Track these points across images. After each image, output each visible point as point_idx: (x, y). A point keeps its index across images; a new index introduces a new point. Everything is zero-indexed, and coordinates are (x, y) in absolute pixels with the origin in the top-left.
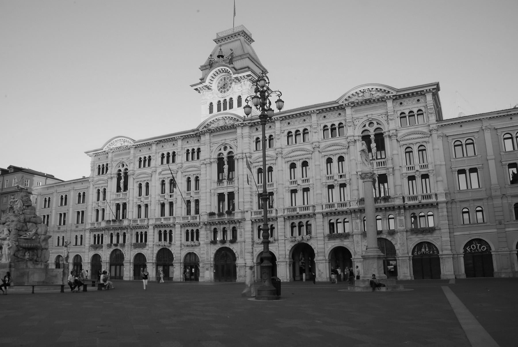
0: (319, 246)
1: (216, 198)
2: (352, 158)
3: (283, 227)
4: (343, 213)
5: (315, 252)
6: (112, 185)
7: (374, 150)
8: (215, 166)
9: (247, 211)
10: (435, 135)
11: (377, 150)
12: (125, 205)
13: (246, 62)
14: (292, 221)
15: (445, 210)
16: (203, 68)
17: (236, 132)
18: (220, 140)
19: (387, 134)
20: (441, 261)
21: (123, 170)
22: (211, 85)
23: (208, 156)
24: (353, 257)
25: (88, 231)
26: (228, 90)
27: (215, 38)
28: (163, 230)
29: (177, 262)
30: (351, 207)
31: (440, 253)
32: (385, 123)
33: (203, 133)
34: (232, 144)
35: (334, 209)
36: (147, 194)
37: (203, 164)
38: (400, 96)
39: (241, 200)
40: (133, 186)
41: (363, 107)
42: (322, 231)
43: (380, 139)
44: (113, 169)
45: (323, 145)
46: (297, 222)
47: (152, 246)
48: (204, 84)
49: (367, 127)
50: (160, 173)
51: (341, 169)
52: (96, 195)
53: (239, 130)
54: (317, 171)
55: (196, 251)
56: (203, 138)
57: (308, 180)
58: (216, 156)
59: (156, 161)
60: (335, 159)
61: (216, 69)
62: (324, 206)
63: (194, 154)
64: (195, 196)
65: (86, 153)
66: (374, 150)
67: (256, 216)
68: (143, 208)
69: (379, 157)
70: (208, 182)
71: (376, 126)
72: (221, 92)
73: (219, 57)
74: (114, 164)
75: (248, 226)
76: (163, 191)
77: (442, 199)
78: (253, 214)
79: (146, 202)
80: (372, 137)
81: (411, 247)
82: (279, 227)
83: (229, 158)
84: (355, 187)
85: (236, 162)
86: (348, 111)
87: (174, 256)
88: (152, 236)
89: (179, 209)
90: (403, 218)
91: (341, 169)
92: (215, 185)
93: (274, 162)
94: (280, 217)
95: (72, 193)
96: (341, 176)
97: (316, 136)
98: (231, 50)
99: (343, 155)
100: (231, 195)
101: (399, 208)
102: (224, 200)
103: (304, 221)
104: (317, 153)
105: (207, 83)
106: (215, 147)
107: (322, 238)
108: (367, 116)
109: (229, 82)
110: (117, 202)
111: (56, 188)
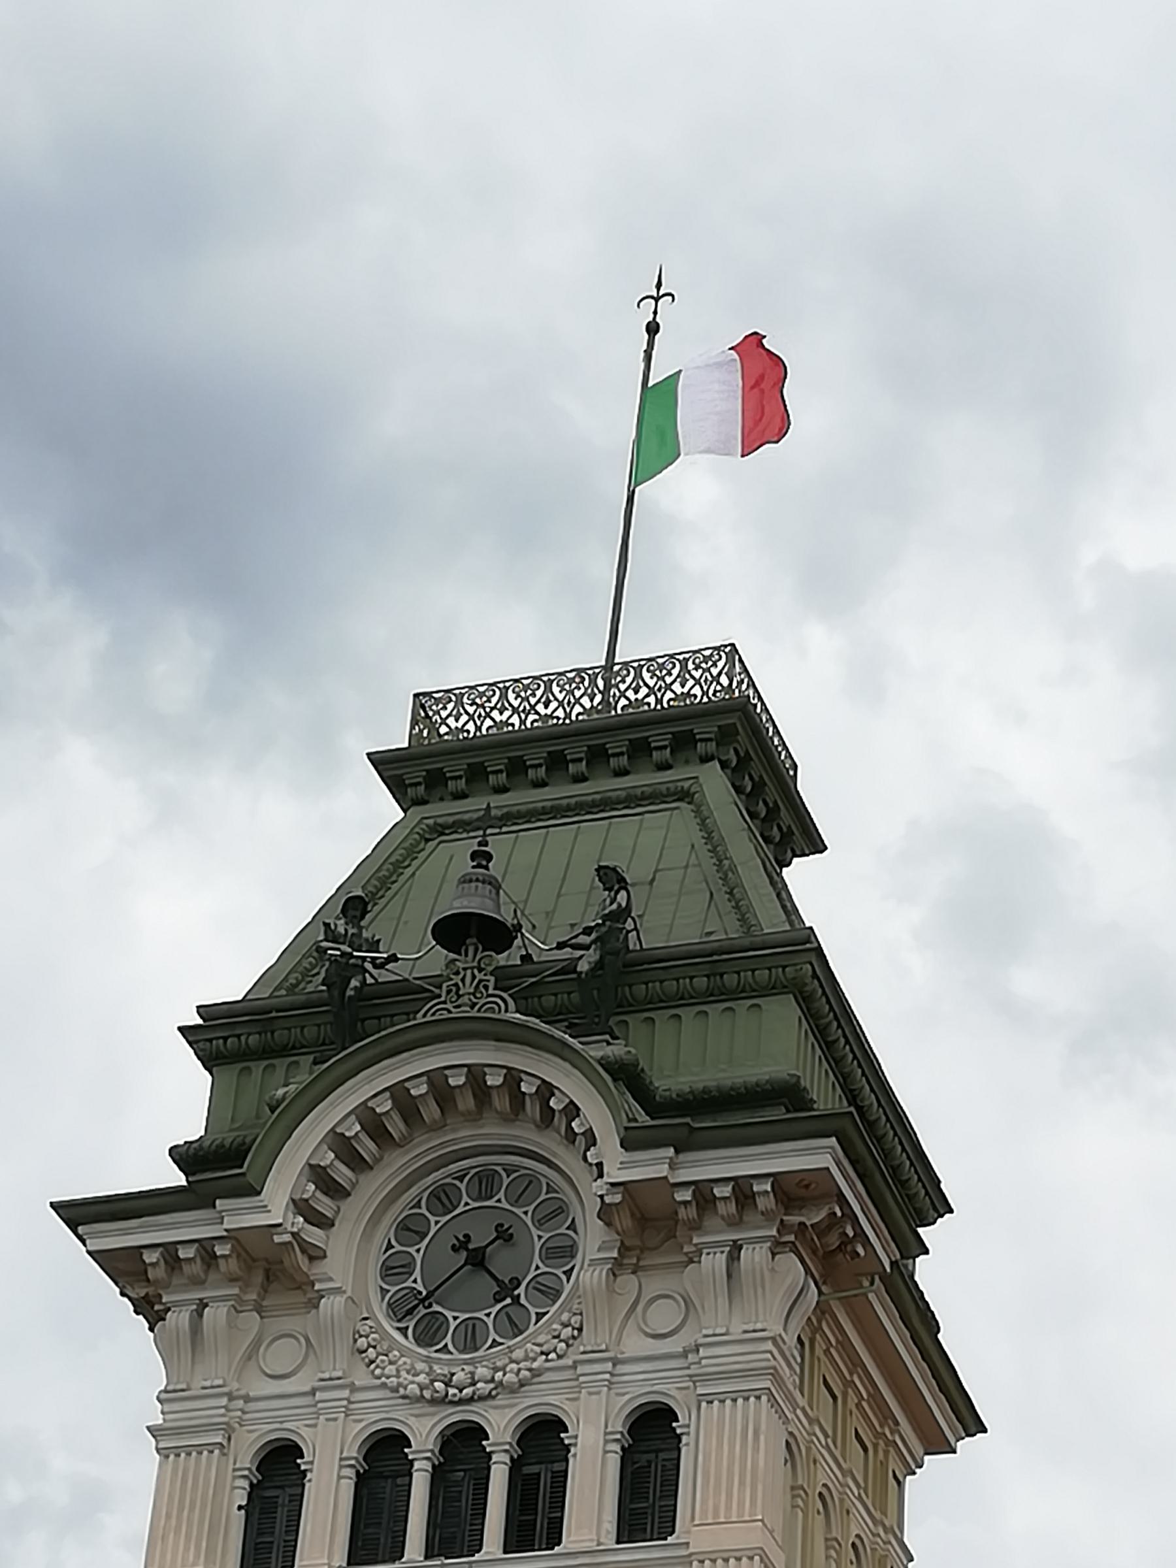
13: (767, 1044)
16: (221, 1037)
22: (314, 1235)
27: (400, 740)
48: (238, 1216)
72: (429, 1334)
73: (453, 932)
98: (611, 878)
109: (538, 1237)
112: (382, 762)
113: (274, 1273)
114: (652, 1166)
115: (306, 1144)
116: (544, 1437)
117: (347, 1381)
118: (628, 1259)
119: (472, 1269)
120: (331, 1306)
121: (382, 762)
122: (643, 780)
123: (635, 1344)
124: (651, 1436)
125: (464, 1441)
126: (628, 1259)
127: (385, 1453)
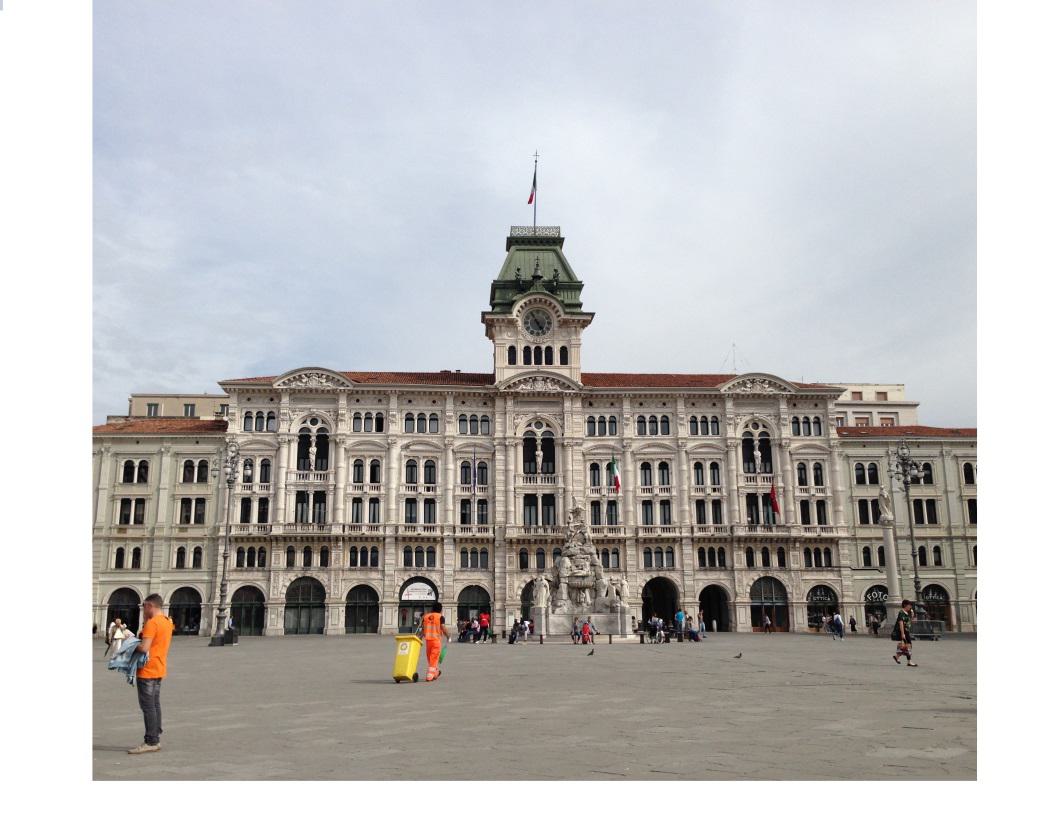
1: (521, 502)
4: (720, 540)
5: (681, 590)
6: (289, 456)
7: (758, 461)
12: (320, 497)
17: (563, 404)
19: (777, 442)
21: (314, 429)
28: (414, 546)
31: (840, 601)
32: (774, 427)
33: (504, 396)
35: (710, 534)
37: (499, 444)
38: (796, 396)
41: (749, 401)
46: (653, 547)
50: (407, 447)
53: (567, 404)
56: (499, 403)
58: (520, 434)
59: (396, 427)
60: (707, 465)
61: (532, 297)
65: (220, 384)
66: (758, 461)
69: (763, 470)
72: (532, 333)
76: (411, 478)
80: (756, 443)
82: (629, 552)
83: (542, 440)
85: (558, 450)
86: (729, 405)
91: (715, 480)
92: (520, 482)
94: (630, 539)
95: (167, 460)
96: (714, 490)
99: (718, 462)
100: (550, 500)
101: (796, 540)
102: (536, 505)
106: (522, 422)
108: (753, 414)
115: (517, 308)
116: (549, 350)
117: (523, 340)
118: (560, 327)
123: (561, 338)
125: (538, 349)
126: (560, 327)
127: (527, 350)
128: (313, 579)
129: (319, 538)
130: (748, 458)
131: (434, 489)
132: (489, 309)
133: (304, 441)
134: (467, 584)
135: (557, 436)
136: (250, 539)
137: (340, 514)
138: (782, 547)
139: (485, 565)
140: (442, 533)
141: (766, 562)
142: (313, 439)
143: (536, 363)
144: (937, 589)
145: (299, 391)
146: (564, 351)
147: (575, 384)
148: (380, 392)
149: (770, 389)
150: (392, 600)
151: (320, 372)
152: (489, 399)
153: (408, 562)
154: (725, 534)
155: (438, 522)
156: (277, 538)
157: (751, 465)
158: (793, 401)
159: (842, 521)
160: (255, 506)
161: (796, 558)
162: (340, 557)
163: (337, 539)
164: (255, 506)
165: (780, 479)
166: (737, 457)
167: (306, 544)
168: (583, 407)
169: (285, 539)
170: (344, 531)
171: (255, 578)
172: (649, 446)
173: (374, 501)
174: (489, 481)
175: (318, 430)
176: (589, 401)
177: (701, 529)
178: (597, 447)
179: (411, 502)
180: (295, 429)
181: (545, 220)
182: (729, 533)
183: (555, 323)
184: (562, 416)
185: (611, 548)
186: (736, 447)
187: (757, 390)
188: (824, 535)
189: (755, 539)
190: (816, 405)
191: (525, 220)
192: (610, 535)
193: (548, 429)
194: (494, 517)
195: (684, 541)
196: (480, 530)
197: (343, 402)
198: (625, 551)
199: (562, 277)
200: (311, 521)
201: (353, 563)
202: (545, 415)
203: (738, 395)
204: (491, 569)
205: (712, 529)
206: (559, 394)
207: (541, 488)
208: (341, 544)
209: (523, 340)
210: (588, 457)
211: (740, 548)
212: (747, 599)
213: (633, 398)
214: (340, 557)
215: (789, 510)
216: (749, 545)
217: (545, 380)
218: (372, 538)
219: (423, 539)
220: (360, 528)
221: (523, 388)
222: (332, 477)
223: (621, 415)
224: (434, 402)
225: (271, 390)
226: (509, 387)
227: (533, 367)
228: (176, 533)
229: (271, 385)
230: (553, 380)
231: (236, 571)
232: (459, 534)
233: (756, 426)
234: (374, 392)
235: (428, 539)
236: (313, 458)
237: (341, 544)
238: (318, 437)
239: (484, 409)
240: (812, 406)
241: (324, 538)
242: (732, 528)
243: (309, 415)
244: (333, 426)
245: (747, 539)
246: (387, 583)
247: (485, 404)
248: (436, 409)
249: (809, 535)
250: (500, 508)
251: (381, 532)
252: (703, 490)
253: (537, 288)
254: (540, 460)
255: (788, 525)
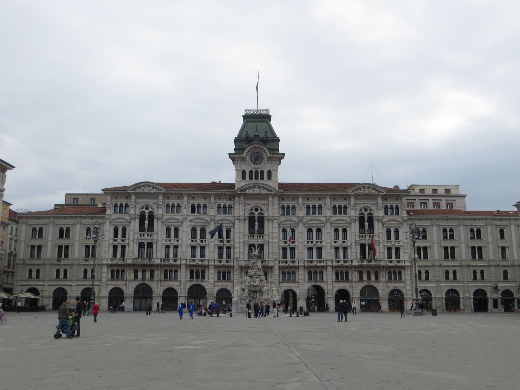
0: (329, 288)
2: (353, 231)
3: (303, 273)
5: (326, 291)
6: (135, 226)
7: (367, 228)
8: (247, 222)
9: (276, 260)
10: (405, 224)
11: (368, 227)
12: (150, 245)
14: (309, 270)
15: (409, 271)
17: (268, 199)
18: (253, 203)
19: (376, 218)
20: (405, 301)
23: (242, 214)
24: (351, 296)
25: (106, 266)
26: (260, 163)
29: (210, 296)
30: (353, 264)
31: (405, 296)
32: (375, 210)
33: (239, 195)
34: (263, 207)
35: (341, 264)
36: (176, 236)
37: (237, 219)
38: (387, 195)
39: (271, 251)
40: (159, 228)
42: (331, 278)
43: (371, 220)
44: (137, 210)
45: (333, 219)
47: (184, 282)
48: (242, 156)
49: (363, 211)
50: (191, 221)
51: (345, 237)
52: (112, 232)
53: (271, 199)
54: (328, 236)
55: (230, 288)
56: (237, 199)
57: (321, 242)
60: (340, 230)
62: (334, 262)
63: (225, 210)
64: (227, 244)
66: (367, 228)
67: (282, 264)
68: (172, 250)
70: (242, 234)
71: (369, 211)
74: (139, 206)
75: (276, 271)
76: (194, 236)
77: (408, 264)
78: (281, 262)
79: (176, 243)
80: (366, 218)
81: (388, 292)
82: (300, 273)
84: (354, 251)
85: (266, 222)
86: (352, 199)
87: (207, 291)
88: (184, 275)
89: (212, 253)
90: (384, 273)
92: (247, 238)
93: (296, 225)
94: (301, 266)
95: (78, 227)
96: (344, 242)
97: (327, 212)
99: (346, 228)
100: (261, 247)
101: (383, 267)
103: (318, 270)
104: (328, 224)
105: (244, 155)
106: (248, 208)
107: (331, 283)
110: (141, 241)
111: (51, 220)
112: (243, 116)
113: (244, 159)
114: (271, 156)
115: (246, 151)
116: (262, 172)
117: (249, 167)
119: (257, 159)
120: (247, 161)
121: (243, 116)
122: (263, 120)
123: (268, 166)
124: (269, 172)
125: (257, 172)
127: (251, 172)
128: (147, 285)
129: (149, 265)
130: (362, 226)
131: (205, 241)
132: (233, 152)
133: (142, 218)
134: (220, 288)
135: (266, 214)
136: (117, 265)
137: (159, 253)
138: (377, 270)
139: (229, 279)
140: (208, 262)
141: (369, 278)
142: (147, 216)
143: (255, 179)
144: (454, 291)
145: (140, 193)
146: (269, 172)
147: (275, 189)
148: (178, 193)
149: (374, 191)
150: (184, 295)
151: (150, 184)
152: (232, 197)
153: (192, 277)
154: (348, 264)
155: (206, 258)
156: (129, 265)
157: (363, 230)
158: (385, 198)
159: (407, 255)
160: (119, 250)
161: (383, 276)
162: (158, 274)
163: (158, 265)
164: (119, 250)
165: (377, 237)
166: (356, 226)
167: (143, 268)
168: (279, 200)
169: (133, 265)
170: (161, 262)
171: (119, 284)
172: (312, 220)
173: (176, 247)
174: (232, 237)
175: (149, 213)
176: (281, 197)
177: (336, 262)
178: (285, 221)
179: (193, 248)
180: (138, 212)
181: (263, 107)
182: (350, 263)
183: (265, 159)
184: (268, 205)
185: (291, 271)
186: (355, 220)
187: (367, 192)
188: (398, 264)
189: (364, 267)
190: (397, 199)
191: (252, 107)
192: (291, 264)
193: (261, 211)
194: (234, 255)
195: (328, 267)
196: (227, 262)
197: (161, 198)
198: (299, 272)
199: (269, 135)
200: (145, 257)
201: (166, 277)
202: (260, 205)
203: (357, 194)
204: (232, 281)
205: (342, 262)
206: (267, 194)
207: (256, 241)
208: (160, 268)
209: (249, 167)
210: (281, 225)
211: (356, 271)
212: (358, 296)
213: (304, 197)
214: (158, 274)
215: (381, 252)
216: (360, 270)
217: (259, 187)
218: (175, 265)
219: (199, 266)
220: (169, 260)
221: (249, 191)
222: (155, 236)
223: (298, 204)
224: (205, 198)
225: (126, 193)
226: (242, 191)
227: (254, 181)
228: (83, 262)
229: (126, 191)
230: (264, 187)
231: (110, 280)
232: (216, 264)
233: (366, 210)
234: (176, 193)
235: (202, 266)
236: (146, 226)
237: (160, 268)
238: (149, 216)
239: (230, 202)
240: (394, 200)
241: (152, 265)
242: (352, 261)
243: (145, 205)
244: (156, 210)
245: (359, 267)
246: (182, 287)
247: (230, 199)
248: (206, 202)
249: (390, 264)
250: (237, 251)
251: (179, 263)
252: (338, 242)
253: (257, 139)
254: (256, 227)
255: (380, 259)
